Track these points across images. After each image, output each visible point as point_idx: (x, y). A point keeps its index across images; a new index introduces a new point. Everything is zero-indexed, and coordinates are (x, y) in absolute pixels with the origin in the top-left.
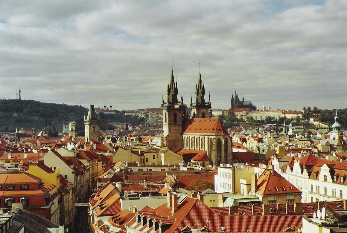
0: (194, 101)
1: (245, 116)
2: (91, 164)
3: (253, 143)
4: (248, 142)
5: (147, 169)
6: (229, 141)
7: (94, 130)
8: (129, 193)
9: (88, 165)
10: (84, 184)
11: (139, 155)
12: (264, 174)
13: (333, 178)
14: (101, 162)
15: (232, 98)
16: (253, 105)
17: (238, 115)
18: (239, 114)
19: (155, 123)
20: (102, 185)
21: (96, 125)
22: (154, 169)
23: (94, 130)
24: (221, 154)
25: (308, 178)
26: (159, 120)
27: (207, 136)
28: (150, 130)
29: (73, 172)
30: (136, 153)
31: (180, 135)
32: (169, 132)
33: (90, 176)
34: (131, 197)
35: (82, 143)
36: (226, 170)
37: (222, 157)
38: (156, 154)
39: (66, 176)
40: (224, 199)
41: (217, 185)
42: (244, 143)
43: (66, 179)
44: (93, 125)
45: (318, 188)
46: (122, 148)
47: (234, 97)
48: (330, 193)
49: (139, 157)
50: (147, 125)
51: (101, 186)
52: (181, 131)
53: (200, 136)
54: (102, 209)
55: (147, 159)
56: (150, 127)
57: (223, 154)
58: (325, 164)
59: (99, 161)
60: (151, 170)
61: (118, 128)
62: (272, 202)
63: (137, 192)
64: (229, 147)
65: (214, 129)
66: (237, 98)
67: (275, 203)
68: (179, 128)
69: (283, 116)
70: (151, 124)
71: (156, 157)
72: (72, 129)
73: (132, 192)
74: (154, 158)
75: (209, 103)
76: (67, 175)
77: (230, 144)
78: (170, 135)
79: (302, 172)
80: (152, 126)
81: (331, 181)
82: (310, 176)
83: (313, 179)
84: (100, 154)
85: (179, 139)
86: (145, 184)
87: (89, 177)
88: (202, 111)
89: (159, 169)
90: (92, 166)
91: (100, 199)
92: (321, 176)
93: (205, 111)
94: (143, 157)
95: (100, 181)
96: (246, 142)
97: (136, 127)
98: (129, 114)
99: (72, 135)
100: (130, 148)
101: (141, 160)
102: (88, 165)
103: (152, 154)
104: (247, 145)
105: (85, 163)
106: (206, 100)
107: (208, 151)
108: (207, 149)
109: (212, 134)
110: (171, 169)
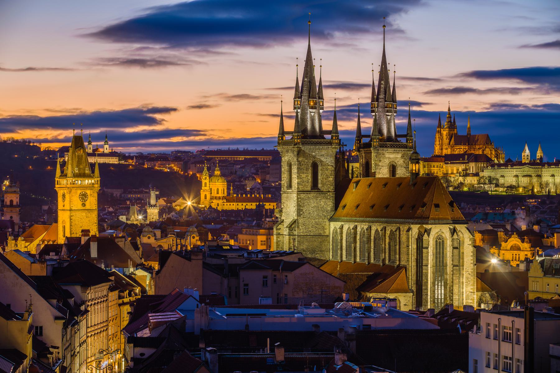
2: (91, 296)
3: (519, 249)
7: (84, 205)
14: (116, 292)
23: (84, 205)
26: (238, 183)
32: (299, 215)
35: (48, 242)
49: (226, 281)
55: (246, 285)
68: (325, 202)
70: (218, 193)
72: (11, 201)
74: (265, 284)
85: (325, 232)
88: (389, 158)
99: (11, 217)
100: (200, 257)
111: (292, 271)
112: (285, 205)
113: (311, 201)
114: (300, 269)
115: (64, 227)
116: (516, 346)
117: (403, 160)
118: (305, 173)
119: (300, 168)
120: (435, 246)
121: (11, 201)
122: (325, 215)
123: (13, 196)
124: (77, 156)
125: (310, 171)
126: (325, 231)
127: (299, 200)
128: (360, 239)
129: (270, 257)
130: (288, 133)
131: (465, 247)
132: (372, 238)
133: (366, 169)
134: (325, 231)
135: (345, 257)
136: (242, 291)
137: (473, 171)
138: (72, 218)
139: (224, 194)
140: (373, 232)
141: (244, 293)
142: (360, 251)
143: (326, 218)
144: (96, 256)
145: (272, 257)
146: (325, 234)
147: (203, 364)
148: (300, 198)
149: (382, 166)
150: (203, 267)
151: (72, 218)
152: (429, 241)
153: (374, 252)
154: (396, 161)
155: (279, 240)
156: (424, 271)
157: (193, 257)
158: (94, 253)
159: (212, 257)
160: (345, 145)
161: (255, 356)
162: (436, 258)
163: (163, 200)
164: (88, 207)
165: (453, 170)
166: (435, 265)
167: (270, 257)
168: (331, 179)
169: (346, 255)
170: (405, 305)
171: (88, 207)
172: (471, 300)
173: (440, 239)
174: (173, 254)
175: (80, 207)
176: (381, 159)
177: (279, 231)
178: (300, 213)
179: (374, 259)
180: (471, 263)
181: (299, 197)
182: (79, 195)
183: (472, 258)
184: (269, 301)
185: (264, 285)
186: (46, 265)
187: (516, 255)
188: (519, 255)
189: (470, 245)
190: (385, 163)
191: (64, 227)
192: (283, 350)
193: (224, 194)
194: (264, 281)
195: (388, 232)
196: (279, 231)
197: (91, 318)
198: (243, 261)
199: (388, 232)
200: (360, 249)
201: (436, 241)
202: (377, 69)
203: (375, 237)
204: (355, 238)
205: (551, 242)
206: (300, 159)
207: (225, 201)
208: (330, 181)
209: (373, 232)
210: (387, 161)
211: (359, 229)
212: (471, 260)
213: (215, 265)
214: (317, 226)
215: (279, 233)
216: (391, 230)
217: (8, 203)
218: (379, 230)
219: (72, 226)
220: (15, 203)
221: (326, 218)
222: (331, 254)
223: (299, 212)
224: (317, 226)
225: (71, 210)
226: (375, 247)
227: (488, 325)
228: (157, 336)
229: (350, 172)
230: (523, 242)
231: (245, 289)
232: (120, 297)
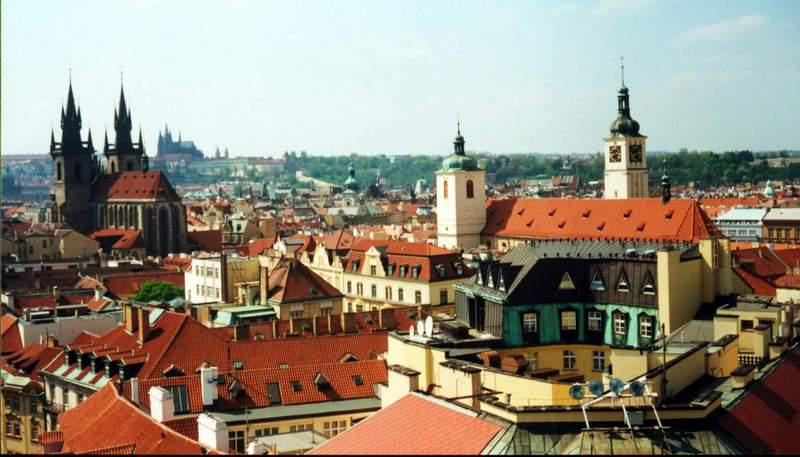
0: (112, 140)
5: (42, 267)
6: (181, 212)
13: (386, 270)
15: (161, 137)
36: (209, 263)
41: (190, 291)
45: (360, 286)
47: (163, 134)
48: (381, 295)
58: (373, 248)
65: (152, 192)
66: (168, 136)
74: (45, 246)
75: (141, 144)
79: (331, 261)
81: (383, 274)
83: (351, 272)
92: (366, 269)
94: (22, 245)
96: (202, 213)
103: (41, 239)
106: (135, 139)
130: (58, 144)
227: (197, 267)
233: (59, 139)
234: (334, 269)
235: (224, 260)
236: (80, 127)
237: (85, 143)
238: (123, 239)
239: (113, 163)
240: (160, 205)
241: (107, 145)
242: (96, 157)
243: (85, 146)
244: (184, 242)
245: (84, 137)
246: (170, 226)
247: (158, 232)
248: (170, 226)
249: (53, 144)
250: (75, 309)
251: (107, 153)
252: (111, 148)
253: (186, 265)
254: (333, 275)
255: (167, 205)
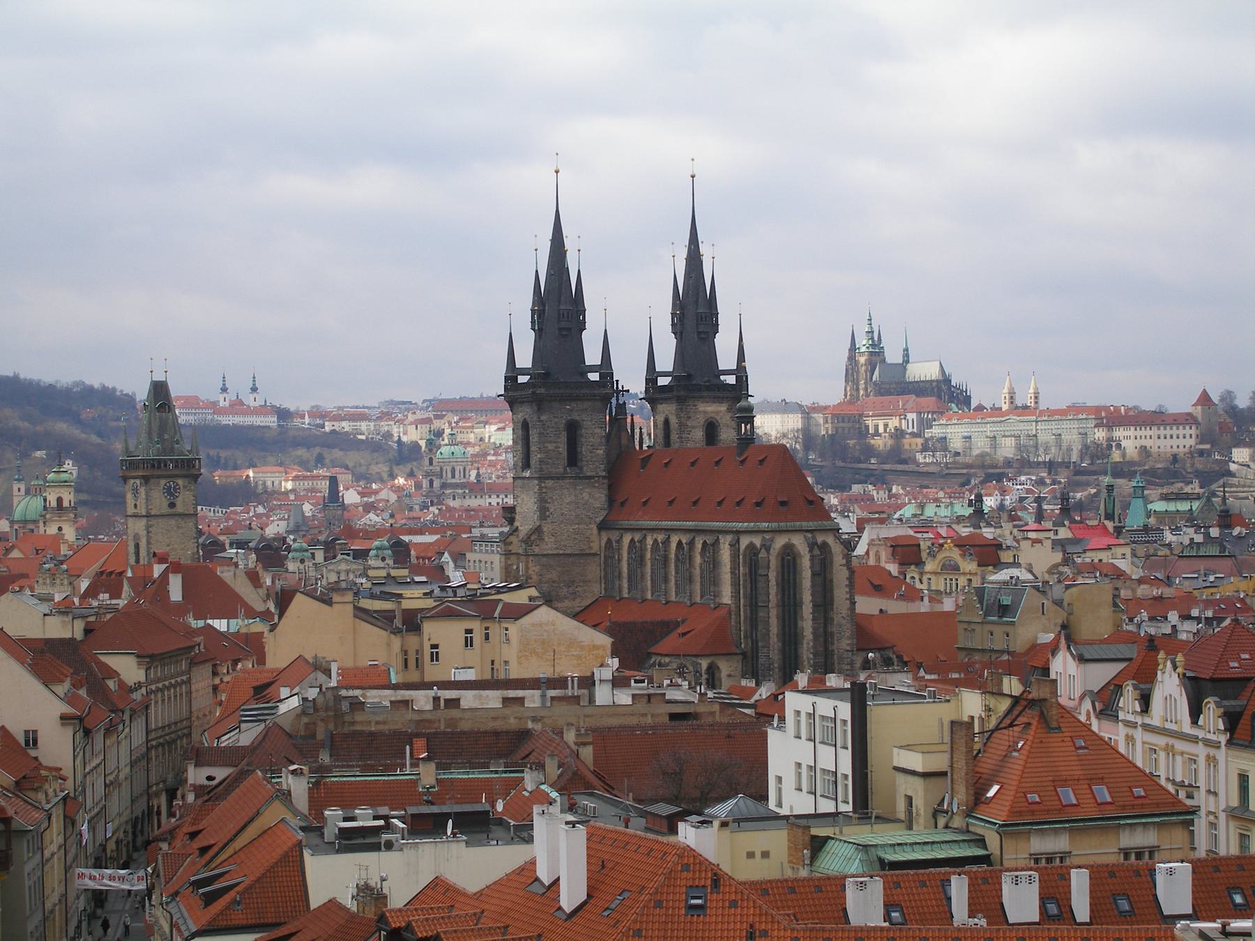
0: (666, 362)
1: (913, 435)
3: (956, 568)
4: (929, 567)
6: (838, 560)
7: (172, 505)
8: (346, 819)
9: (143, 679)
10: (122, 776)
11: (396, 632)
12: (1007, 721)
15: (853, 348)
16: (953, 383)
17: (881, 430)
18: (886, 426)
19: (474, 473)
20: (210, 778)
21: (180, 482)
22: (469, 699)
23: (172, 505)
24: (800, 623)
25: (1223, 743)
26: (494, 458)
27: (729, 538)
28: (448, 508)
29: (64, 718)
30: (384, 620)
31: (595, 531)
33: (153, 735)
34: (354, 841)
36: (825, 706)
37: (803, 637)
38: (476, 625)
39: (32, 739)
40: (818, 845)
41: (779, 779)
42: (912, 572)
43: (33, 753)
44: (163, 482)
46: (311, 595)
47: (863, 343)
49: (396, 642)
50: (431, 482)
51: (206, 782)
52: (604, 513)
53: (693, 534)
54: (210, 899)
55: (435, 646)
56: (448, 491)
57: (807, 625)
59: (193, 663)
60: (453, 703)
61: (292, 497)
62: (1139, 855)
63: (384, 810)
64: (840, 593)
67: (1151, 857)
68: (590, 494)
69: (1100, 434)
70: (453, 476)
71: (477, 637)
72: (60, 500)
73: (365, 818)
74: (469, 643)
76: (35, 732)
77: (840, 575)
78: (545, 529)
79: (1195, 712)
80: (456, 486)
82: (1231, 735)
84: (201, 623)
85: (591, 548)
86: (428, 775)
87: (148, 741)
88: (705, 412)
89: (492, 699)
90: (160, 685)
91: (203, 850)
93: (718, 412)
94: (412, 640)
95: (201, 757)
96: (919, 563)
97: (376, 492)
98: (346, 426)
99: (60, 529)
101: (406, 653)
102: (143, 679)
104: (925, 578)
105: (127, 668)
106: (726, 359)
107: (733, 606)
108: (726, 598)
109: (752, 524)
110: (553, 698)
111: (517, 619)
112: (519, 499)
113: (565, 491)
114: (530, 615)
115: (137, 546)
116: (841, 752)
117: (730, 414)
118: (554, 442)
119: (543, 433)
120: (780, 569)
121: (60, 500)
122: (591, 516)
123: (62, 491)
124: (158, 417)
125: (563, 438)
126: (592, 544)
127: (544, 490)
128: (651, 559)
129: (478, 594)
130: (523, 372)
131: (834, 569)
132: (673, 556)
133: (665, 433)
134: (592, 544)
135: (627, 591)
136: (427, 657)
137: (913, 428)
138: (150, 529)
139: (464, 477)
140: (674, 546)
141: (432, 660)
142: (652, 580)
143: (592, 522)
144: (181, 599)
145: (482, 595)
146: (593, 551)
147: (277, 796)
148: (546, 487)
149: (693, 427)
150: (355, 616)
151: (150, 529)
152: (769, 561)
153: (676, 581)
154: (718, 418)
155: (509, 562)
156: (761, 614)
157: (336, 598)
158: (175, 590)
159: (373, 597)
160: (626, 391)
161: (384, 778)
162: (783, 590)
163: (355, 490)
164: (180, 509)
165: (876, 427)
166: (781, 604)
167: (478, 594)
168: (601, 452)
169: (629, 589)
170: (729, 676)
171: (180, 509)
172: (848, 664)
173: (788, 555)
174: (298, 594)
175: (165, 510)
176: (691, 414)
177: (510, 548)
178: (545, 513)
179: (677, 595)
180: (847, 599)
181: (543, 485)
182: (164, 488)
183: (848, 590)
184: (470, 675)
185: (467, 646)
186: (71, 618)
187: (951, 580)
188: (957, 580)
189: (844, 565)
190: (698, 421)
191: (137, 546)
192: (432, 766)
193: (464, 477)
194: (466, 638)
195: (699, 546)
196: (510, 548)
197: (162, 709)
198: (430, 603)
199: (699, 546)
200: (652, 576)
201: (783, 560)
202: (682, 254)
203: (676, 556)
204: (642, 558)
205: (1015, 556)
206: (543, 418)
207: (467, 491)
208: (598, 455)
209: (674, 546)
210: (700, 420)
211: (649, 541)
212: (847, 593)
213: (375, 611)
214: (576, 536)
215: (510, 551)
216: (705, 543)
217: (54, 504)
218: (684, 541)
219: (151, 544)
220: (66, 504)
221: (592, 522)
222: (603, 585)
223: (543, 512)
224: (576, 536)
225: (148, 516)
226: (677, 573)
227: (798, 713)
228: (247, 744)
229: (637, 437)
230: (963, 556)
231: (432, 653)
232: (215, 674)
233: (525, 359)
234: (1201, 734)
235: (859, 698)
236: (582, 326)
237: (593, 369)
238: (680, 630)
239: (667, 422)
240: (780, 542)
241: (652, 374)
242: (622, 408)
243: (594, 377)
244: (844, 643)
245: (592, 356)
246: (807, 597)
247: (773, 613)
248: (807, 597)
249: (512, 371)
250: (446, 816)
251: (654, 394)
252: (663, 381)
253: (771, 713)
254: (1201, 751)
255: (799, 542)
